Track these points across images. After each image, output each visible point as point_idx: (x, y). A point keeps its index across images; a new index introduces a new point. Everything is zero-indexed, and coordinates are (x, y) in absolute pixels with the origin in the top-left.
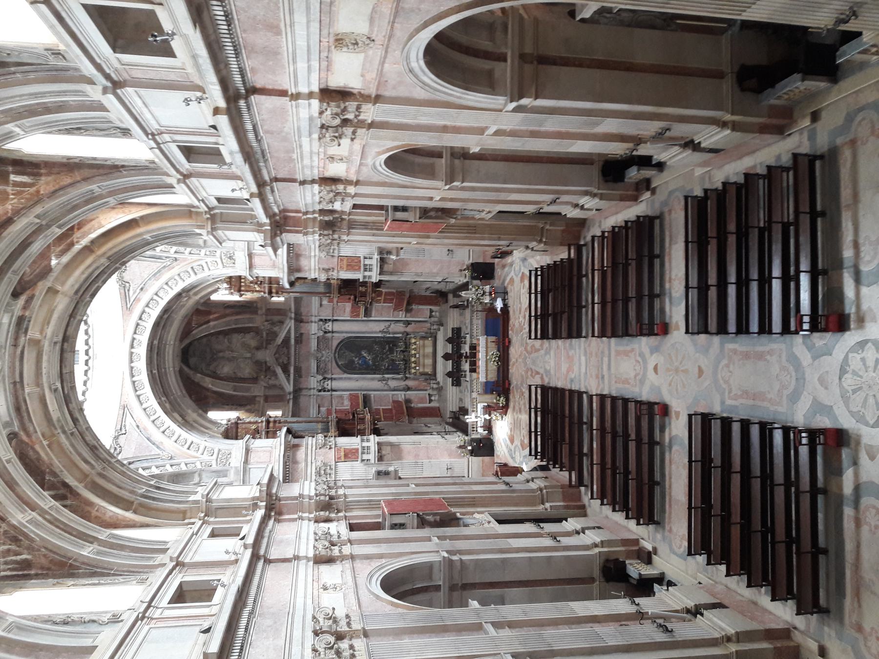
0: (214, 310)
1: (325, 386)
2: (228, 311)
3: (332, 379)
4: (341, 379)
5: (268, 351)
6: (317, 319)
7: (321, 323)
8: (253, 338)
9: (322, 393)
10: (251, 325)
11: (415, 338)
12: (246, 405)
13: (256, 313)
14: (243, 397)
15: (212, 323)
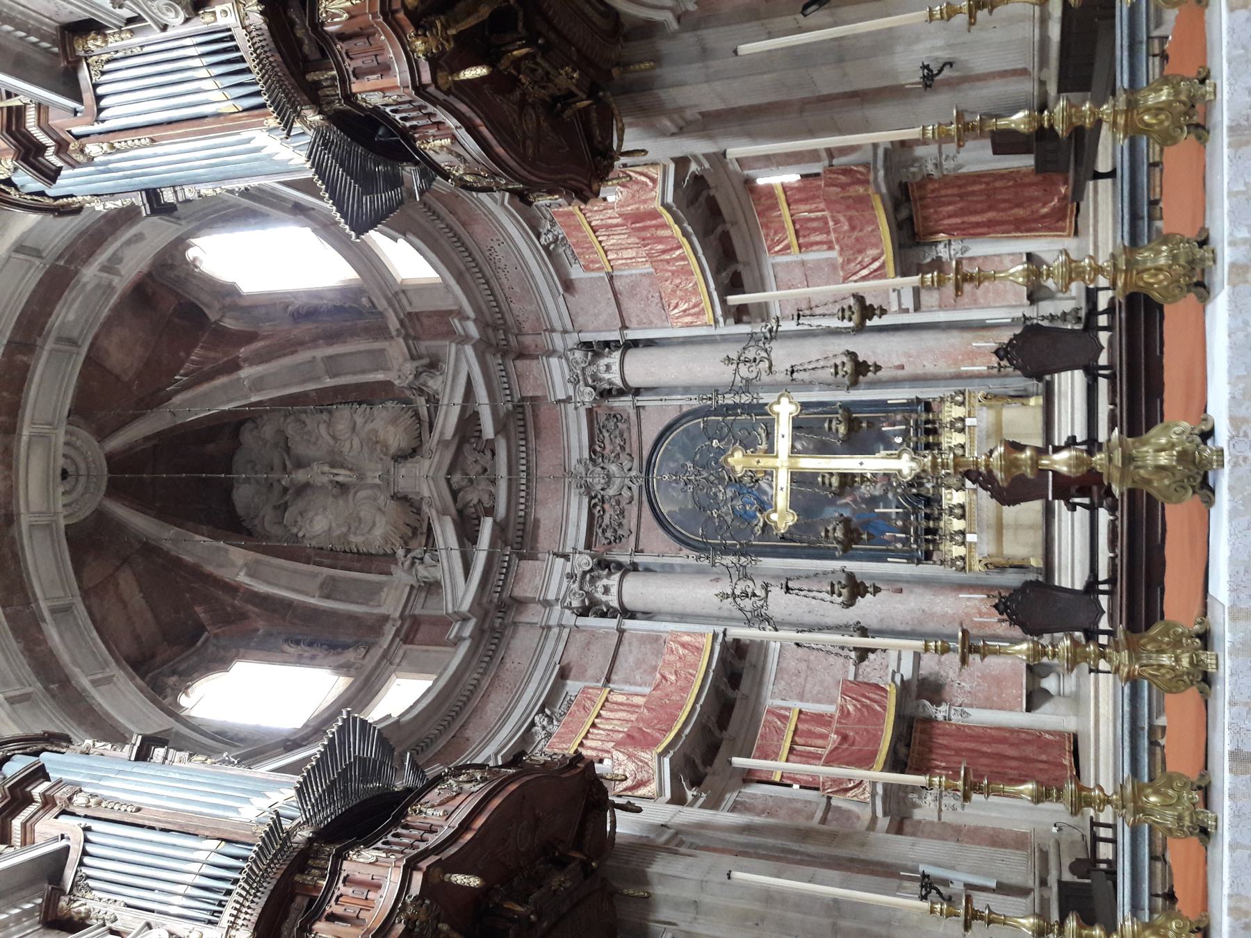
0: (266, 328)
1: (599, 595)
2: (305, 329)
3: (634, 567)
4: (668, 569)
5: (427, 463)
6: (573, 339)
7: (579, 355)
8: (394, 421)
9: (591, 621)
10: (380, 376)
11: (961, 399)
12: (345, 647)
13: (381, 332)
14: (352, 617)
15: (246, 372)
